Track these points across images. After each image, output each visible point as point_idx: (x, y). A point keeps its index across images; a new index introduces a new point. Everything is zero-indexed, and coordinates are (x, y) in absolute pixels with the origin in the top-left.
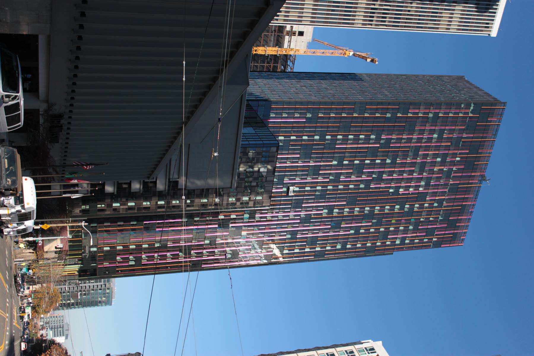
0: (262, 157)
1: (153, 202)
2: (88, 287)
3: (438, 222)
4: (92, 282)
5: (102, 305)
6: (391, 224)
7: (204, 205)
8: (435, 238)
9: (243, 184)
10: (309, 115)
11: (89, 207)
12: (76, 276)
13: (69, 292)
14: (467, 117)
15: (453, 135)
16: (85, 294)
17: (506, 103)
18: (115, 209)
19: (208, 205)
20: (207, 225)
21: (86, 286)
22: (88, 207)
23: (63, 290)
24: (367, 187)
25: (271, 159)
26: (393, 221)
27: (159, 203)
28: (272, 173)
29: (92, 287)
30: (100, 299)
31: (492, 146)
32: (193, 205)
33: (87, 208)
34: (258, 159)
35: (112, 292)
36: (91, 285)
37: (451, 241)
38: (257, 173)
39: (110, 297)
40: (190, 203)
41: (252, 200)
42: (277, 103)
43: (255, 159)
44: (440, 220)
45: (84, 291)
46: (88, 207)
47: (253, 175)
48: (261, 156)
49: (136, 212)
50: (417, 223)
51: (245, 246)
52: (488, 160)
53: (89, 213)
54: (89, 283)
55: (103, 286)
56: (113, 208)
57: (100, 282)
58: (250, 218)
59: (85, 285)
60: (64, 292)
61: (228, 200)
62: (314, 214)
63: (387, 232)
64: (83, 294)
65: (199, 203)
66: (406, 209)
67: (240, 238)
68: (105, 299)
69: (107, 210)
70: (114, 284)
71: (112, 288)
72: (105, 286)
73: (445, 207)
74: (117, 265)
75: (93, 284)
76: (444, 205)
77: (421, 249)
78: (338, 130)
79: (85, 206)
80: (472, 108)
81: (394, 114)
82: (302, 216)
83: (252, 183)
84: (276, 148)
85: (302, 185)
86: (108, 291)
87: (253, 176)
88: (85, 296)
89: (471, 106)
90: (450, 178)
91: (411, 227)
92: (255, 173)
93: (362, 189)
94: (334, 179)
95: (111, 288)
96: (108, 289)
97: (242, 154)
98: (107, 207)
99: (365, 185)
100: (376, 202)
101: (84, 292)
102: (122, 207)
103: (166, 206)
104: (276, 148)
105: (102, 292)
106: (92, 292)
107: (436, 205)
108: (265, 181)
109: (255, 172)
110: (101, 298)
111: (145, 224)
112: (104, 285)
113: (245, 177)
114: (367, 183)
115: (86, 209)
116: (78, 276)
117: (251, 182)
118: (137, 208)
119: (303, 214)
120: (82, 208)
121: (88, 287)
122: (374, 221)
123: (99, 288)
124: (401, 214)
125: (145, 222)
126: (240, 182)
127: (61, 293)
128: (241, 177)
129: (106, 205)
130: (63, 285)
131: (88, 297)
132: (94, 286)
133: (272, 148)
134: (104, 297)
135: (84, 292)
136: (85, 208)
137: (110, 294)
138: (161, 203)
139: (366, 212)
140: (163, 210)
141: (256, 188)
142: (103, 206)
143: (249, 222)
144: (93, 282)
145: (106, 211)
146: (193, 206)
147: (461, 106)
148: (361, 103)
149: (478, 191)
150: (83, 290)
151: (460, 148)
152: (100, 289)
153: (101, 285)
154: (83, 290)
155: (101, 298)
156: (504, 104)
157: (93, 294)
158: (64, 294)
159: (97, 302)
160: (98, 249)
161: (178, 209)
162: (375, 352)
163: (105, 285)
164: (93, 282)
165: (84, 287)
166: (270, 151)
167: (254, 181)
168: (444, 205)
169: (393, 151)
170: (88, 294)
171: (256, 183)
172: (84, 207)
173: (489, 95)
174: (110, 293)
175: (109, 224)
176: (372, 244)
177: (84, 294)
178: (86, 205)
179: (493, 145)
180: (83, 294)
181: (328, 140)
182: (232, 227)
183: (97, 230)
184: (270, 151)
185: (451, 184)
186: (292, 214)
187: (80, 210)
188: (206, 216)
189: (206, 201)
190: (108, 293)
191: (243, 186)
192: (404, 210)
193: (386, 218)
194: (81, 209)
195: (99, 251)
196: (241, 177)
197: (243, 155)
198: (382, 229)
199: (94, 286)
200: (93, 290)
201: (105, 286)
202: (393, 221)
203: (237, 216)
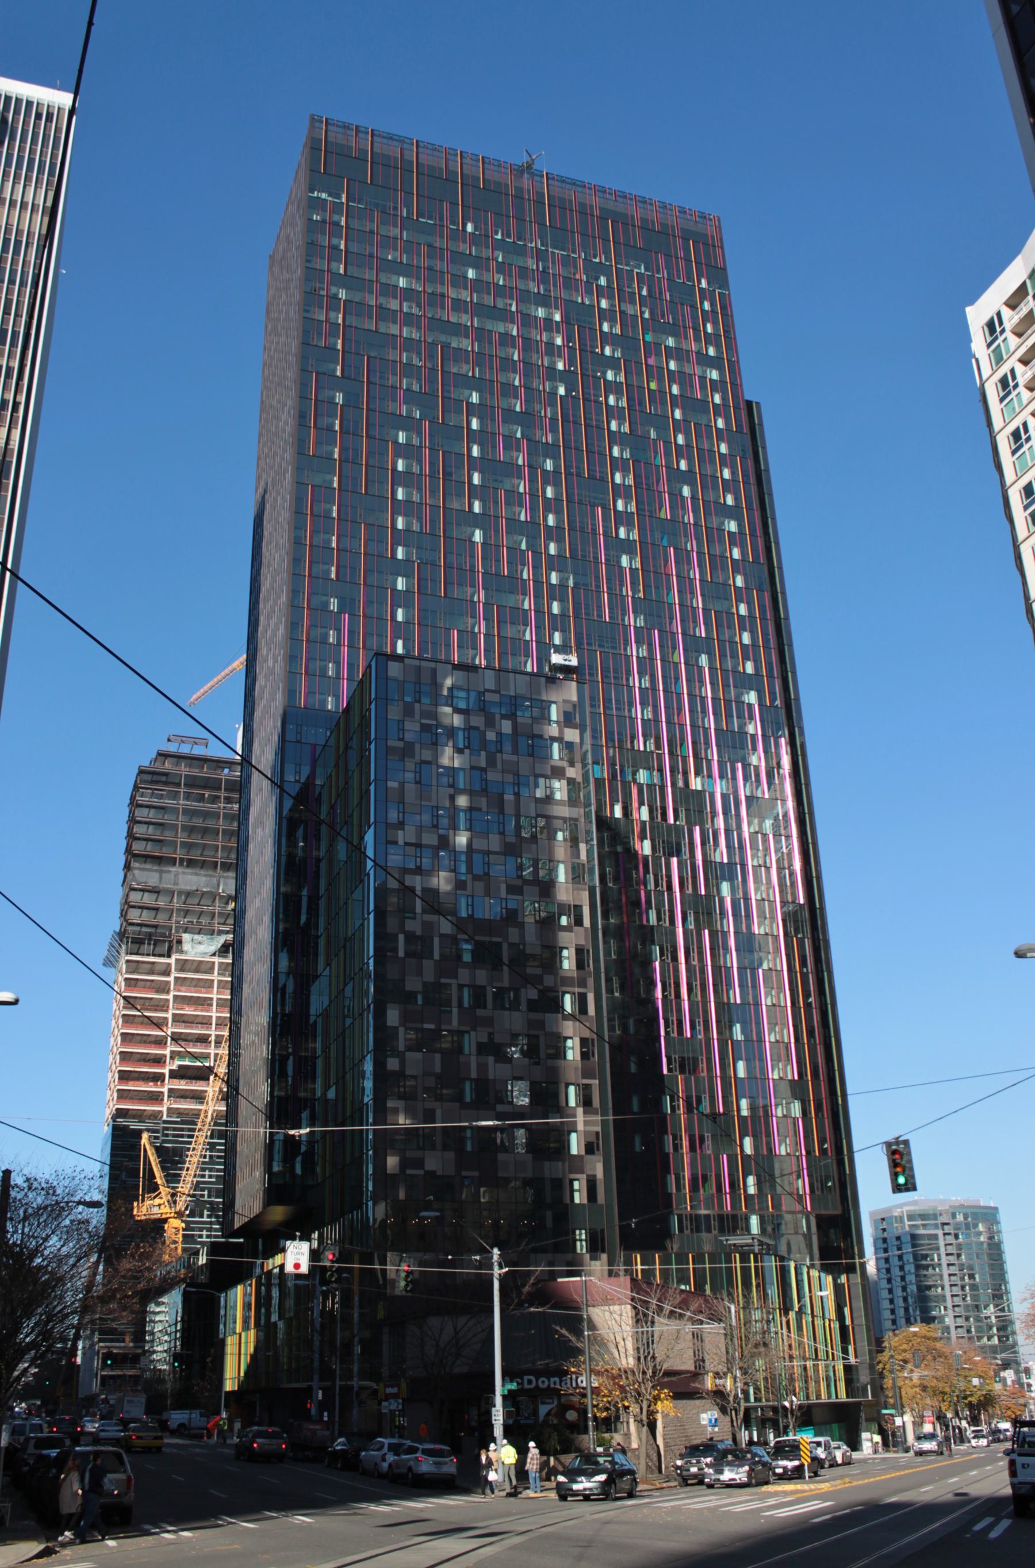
0: (419, 701)
1: (569, 1028)
2: (951, 1268)
3: (653, 276)
4: (939, 1260)
5: (999, 1232)
6: (661, 392)
7: (577, 874)
8: (699, 282)
9: (506, 757)
10: (334, 605)
11: (580, 1229)
12: (851, 1281)
13: (967, 1319)
14: (347, 205)
15: (546, 416)
16: (972, 1276)
18: (590, 1148)
19: (576, 861)
20: (670, 887)
21: (950, 1275)
22: (580, 1234)
23: (962, 1332)
24: (551, 451)
25: (426, 678)
26: (653, 386)
27: (568, 1007)
28: (471, 674)
29: (951, 1258)
30: (982, 1239)
31: (435, 150)
32: (575, 906)
33: (583, 1237)
34: (425, 714)
35: (962, 1206)
36: (944, 1261)
37: (706, 244)
39: (975, 1210)
40: (569, 916)
41: (561, 732)
42: (291, 693)
43: (423, 721)
44: (646, 269)
45: (962, 1279)
46: (582, 1235)
47: (477, 728)
48: (417, 705)
49: (597, 1082)
50: (653, 325)
51: (734, 778)
52: (474, 157)
53: (602, 1231)
54: (940, 1265)
55: (947, 1229)
56: (583, 1153)
57: (937, 1239)
58: (650, 768)
59: (946, 1277)
60: (969, 1331)
61: (560, 803)
62: (635, 591)
63: (684, 401)
64: (972, 1282)
65: (567, 890)
66: (618, 354)
67: (712, 796)
68: (980, 1225)
69: (590, 1173)
70: (942, 1201)
71: (951, 1207)
72: (948, 1224)
73: (608, 259)
74: (804, 1152)
75: (943, 1256)
76: (603, 261)
77: (732, 316)
78: (378, 532)
79: (578, 1243)
80: (324, 196)
81: (337, 384)
82: (641, 622)
83: (503, 731)
84: (390, 663)
85: (546, 623)
86: (960, 1218)
87: (482, 728)
88: (977, 1276)
89: (318, 198)
90: (525, 245)
91: (671, 342)
92: (472, 724)
93: (556, 466)
94: (527, 537)
95: (952, 1210)
96: (954, 1215)
97: (406, 759)
98: (583, 1173)
99: (546, 456)
100: (595, 429)
101: (966, 1278)
102: (580, 1127)
103: (577, 990)
105: (964, 1230)
106: (963, 1257)
107: (603, 281)
108: (498, 695)
109: (467, 721)
110: (979, 1234)
111: (670, 1070)
112: (946, 1227)
113: (483, 753)
114: (537, 450)
115: (586, 1240)
116: (851, 1275)
117: (500, 734)
118: (583, 1077)
119: (634, 621)
120: (584, 1251)
121: (953, 1270)
122: (653, 435)
123: (954, 1241)
124: (631, 366)
125: (665, 1071)
126: (499, 766)
127: (970, 1338)
128: (483, 765)
129: (573, 1176)
130: (949, 1333)
131: (977, 1268)
132: (947, 1255)
134: (976, 1226)
135: (966, 1278)
136: (584, 1243)
137: (969, 1211)
138: (568, 1003)
139: (627, 455)
140: (591, 998)
141: (519, 720)
142: (576, 1185)
143: (661, 770)
144: (939, 1255)
145: (595, 1176)
146: (578, 908)
147: (317, 221)
148: (299, 469)
149: (564, 181)
150: (959, 1283)
151: (438, 222)
152: (956, 1236)
153: (945, 1234)
154: (959, 1283)
155: (979, 1234)
156: (314, 120)
157: (969, 1256)
158: (973, 1329)
159: (989, 1244)
160: (753, 1212)
161: (588, 951)
162: (999, 314)
163: (944, 1224)
164: (939, 1255)
165: (953, 1278)
166: (401, 679)
167: (497, 727)
168: (603, 261)
169: (446, 388)
170: (971, 1268)
171: (504, 722)
172: (582, 1246)
173: (299, 165)
174: (965, 1210)
175: (672, 1179)
176: (720, 439)
177: (970, 1278)
178: (575, 1240)
179: (430, 146)
180: (972, 1282)
181: (407, 553)
182: (676, 817)
183: (691, 1215)
185: (542, 245)
186: (635, 651)
187: (592, 1259)
188: (643, 893)
189: (561, 869)
190: (965, 1218)
191: (514, 758)
192: (619, 359)
193: (641, 403)
194: (588, 1256)
195: (760, 1209)
196: (483, 765)
197: (413, 756)
198: (678, 415)
199: (947, 1255)
200: (959, 1255)
201: (948, 1224)
202: (653, 386)
203: (641, 803)
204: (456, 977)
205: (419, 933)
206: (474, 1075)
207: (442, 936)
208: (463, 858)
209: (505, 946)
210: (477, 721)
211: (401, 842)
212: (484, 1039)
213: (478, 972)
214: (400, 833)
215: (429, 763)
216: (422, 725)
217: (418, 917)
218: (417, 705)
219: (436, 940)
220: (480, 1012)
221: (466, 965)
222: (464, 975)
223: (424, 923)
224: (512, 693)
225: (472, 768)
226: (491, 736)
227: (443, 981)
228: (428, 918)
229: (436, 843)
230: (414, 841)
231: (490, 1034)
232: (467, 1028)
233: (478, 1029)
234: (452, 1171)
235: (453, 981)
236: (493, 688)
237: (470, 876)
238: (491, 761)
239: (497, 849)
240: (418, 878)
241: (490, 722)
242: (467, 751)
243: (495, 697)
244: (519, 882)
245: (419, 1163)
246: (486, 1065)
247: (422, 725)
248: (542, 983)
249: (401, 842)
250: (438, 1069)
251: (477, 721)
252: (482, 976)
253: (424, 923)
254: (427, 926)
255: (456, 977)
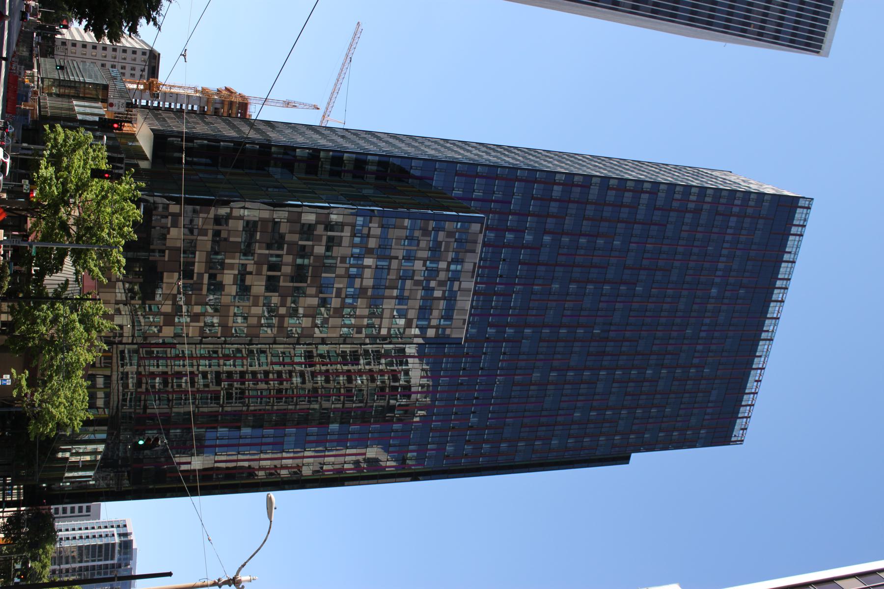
17: (812, 199)
38: (444, 273)
43: (444, 243)
87: (438, 279)
104: (479, 225)
109: (443, 270)
117: (433, 289)
128: (415, 278)
133: (473, 224)
166: (470, 231)
167: (439, 288)
184: (470, 231)
196: (415, 278)
197: (422, 236)
204: (287, 254)
205: (315, 233)
206: (227, 261)
207: (313, 246)
208: (360, 262)
209: (305, 285)
210: (442, 276)
211: (371, 225)
212: (250, 268)
213: (290, 267)
214: (377, 225)
215: (418, 245)
216: (441, 242)
217: (325, 233)
218: (453, 240)
219: (310, 243)
220: (265, 267)
221: (294, 260)
222: (288, 259)
223: (321, 236)
224: (458, 299)
225: (414, 271)
226: (433, 284)
227: (286, 246)
228: (324, 239)
229: (370, 246)
230: (372, 233)
231: (251, 273)
232: (256, 259)
233: (255, 265)
234: (169, 243)
235: (285, 252)
236: (462, 287)
237: (348, 266)
238: (417, 283)
239: (364, 284)
240: (349, 234)
241: (441, 284)
242: (424, 268)
243: (456, 288)
244: (343, 296)
245: (175, 224)
246: (232, 269)
247: (441, 242)
248: (282, 306)
249: (371, 225)
250: (232, 239)
251: (442, 276)
252: (287, 270)
253: (321, 236)
254: (319, 238)
255: (287, 254)
